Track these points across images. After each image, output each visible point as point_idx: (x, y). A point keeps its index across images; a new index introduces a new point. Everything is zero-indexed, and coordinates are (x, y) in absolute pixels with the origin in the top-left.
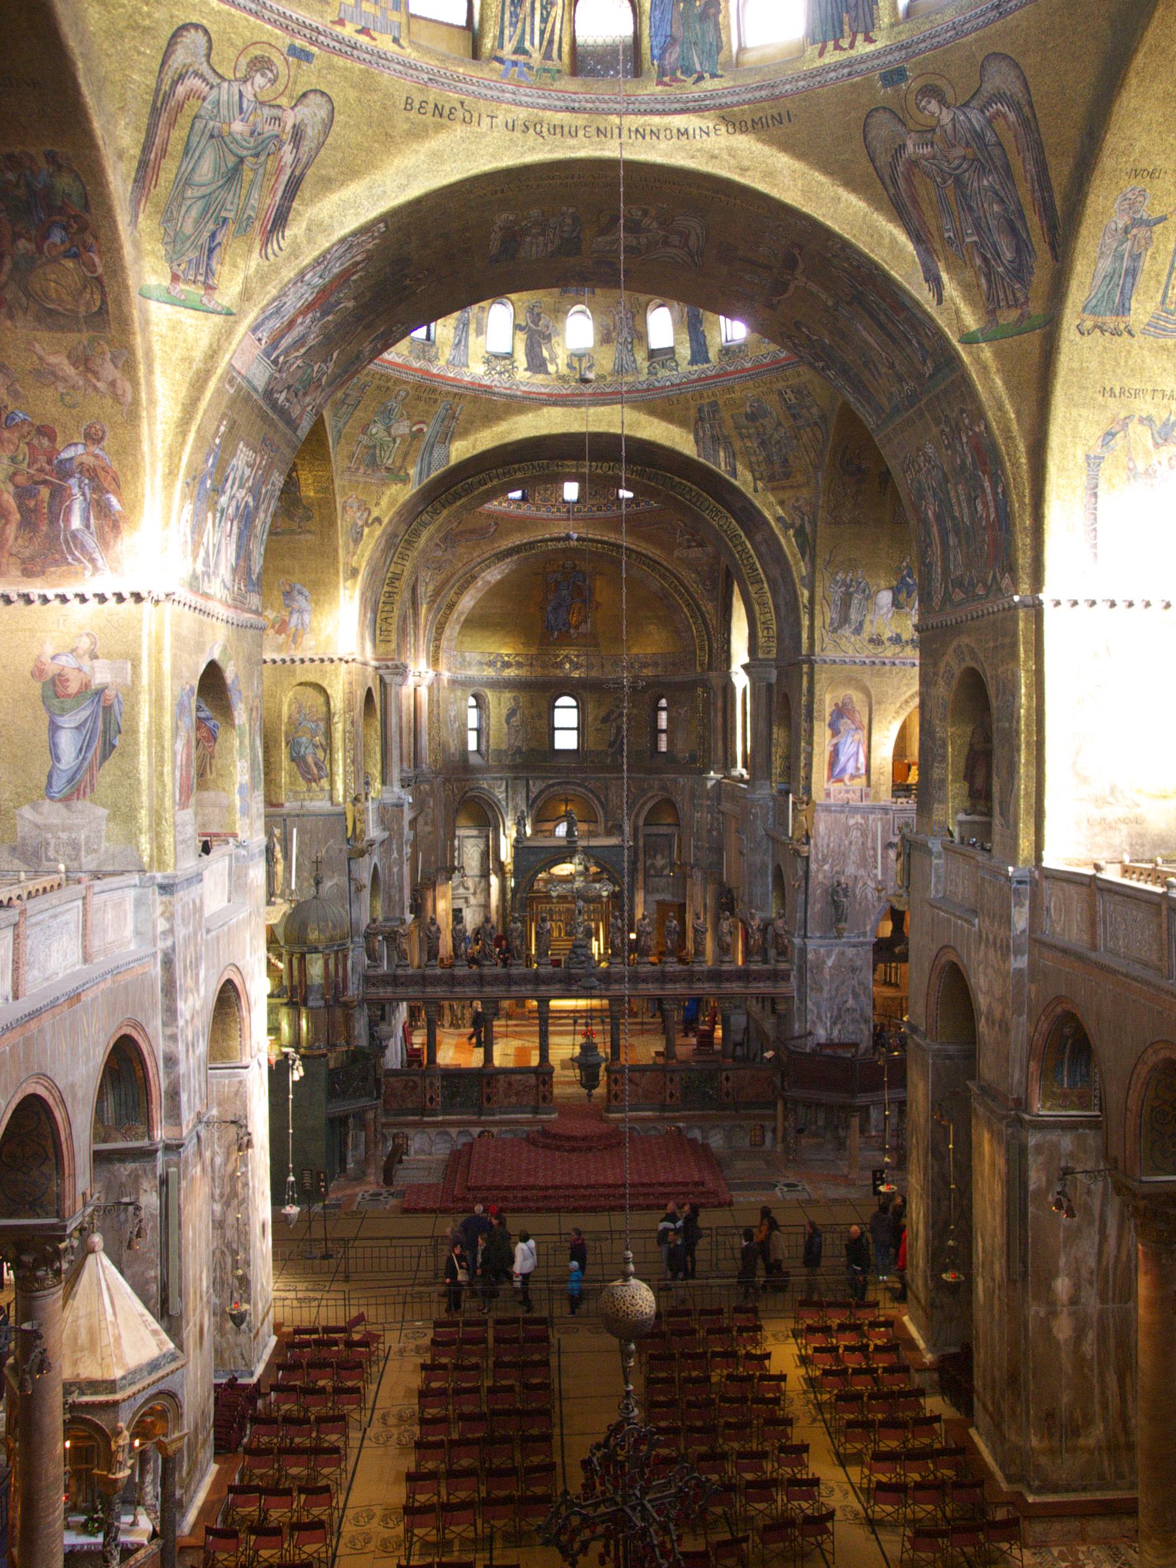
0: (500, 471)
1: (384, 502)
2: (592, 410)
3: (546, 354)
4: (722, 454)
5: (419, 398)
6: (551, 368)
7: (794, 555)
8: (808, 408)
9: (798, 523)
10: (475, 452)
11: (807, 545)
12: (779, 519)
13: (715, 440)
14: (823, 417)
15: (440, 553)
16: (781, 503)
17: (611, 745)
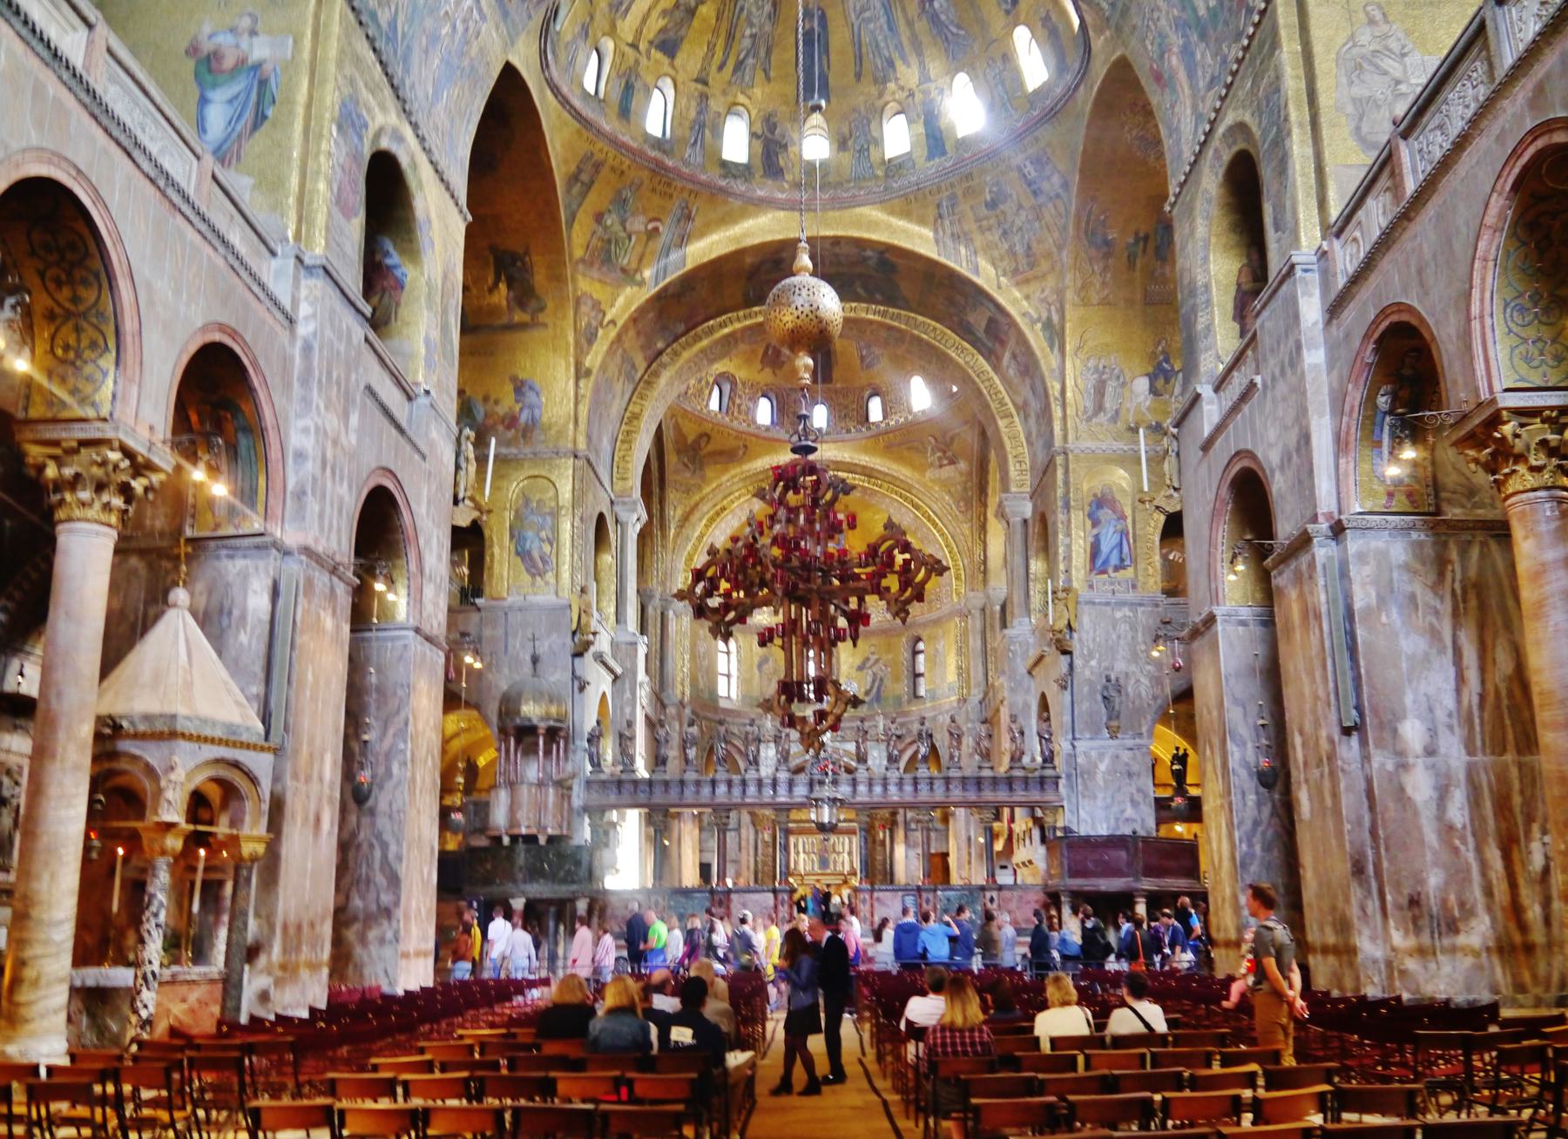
0: (741, 313)
1: (621, 300)
2: (831, 214)
3: (782, 162)
4: (963, 250)
5: (654, 190)
6: (788, 177)
7: (1043, 350)
8: (1049, 178)
9: (1045, 315)
10: (714, 256)
11: (1055, 334)
12: (1024, 315)
13: (956, 237)
14: (1065, 185)
15: (688, 475)
16: (1027, 297)
17: (867, 693)
